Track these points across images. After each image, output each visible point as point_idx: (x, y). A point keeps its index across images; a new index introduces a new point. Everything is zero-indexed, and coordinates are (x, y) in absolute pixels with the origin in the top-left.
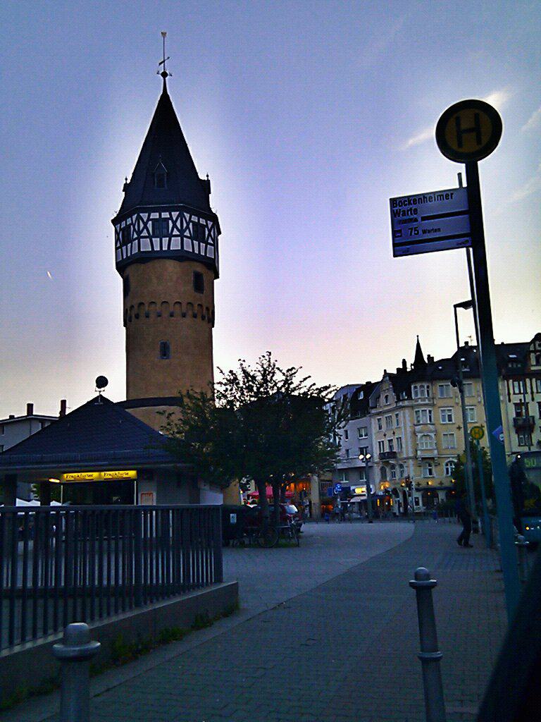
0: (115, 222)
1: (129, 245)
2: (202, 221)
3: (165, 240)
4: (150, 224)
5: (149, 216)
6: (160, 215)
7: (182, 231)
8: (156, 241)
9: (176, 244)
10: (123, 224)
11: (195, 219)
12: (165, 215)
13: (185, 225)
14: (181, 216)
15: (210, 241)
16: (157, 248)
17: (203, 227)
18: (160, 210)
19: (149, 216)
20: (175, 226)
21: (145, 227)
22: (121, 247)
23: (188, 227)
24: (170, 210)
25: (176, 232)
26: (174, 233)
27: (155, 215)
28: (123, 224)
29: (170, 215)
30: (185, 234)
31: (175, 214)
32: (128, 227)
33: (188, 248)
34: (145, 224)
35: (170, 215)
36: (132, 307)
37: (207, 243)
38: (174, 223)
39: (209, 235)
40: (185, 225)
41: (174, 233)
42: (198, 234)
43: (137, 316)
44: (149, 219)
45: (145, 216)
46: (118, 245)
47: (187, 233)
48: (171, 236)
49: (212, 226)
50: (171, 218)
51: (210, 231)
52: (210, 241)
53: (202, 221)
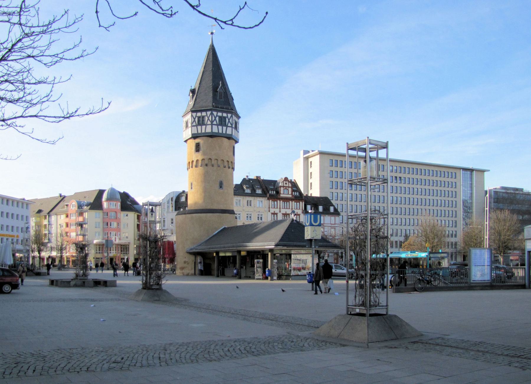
2: (225, 115)
3: (204, 127)
7: (212, 122)
8: (199, 127)
9: (209, 129)
11: (220, 114)
12: (204, 114)
14: (212, 114)
15: (229, 125)
16: (200, 132)
17: (225, 118)
20: (208, 119)
23: (215, 119)
25: (209, 123)
27: (199, 114)
33: (215, 130)
37: (227, 126)
39: (229, 121)
40: (214, 118)
42: (222, 122)
47: (215, 123)
49: (232, 116)
51: (229, 120)
52: (229, 125)
53: (225, 115)
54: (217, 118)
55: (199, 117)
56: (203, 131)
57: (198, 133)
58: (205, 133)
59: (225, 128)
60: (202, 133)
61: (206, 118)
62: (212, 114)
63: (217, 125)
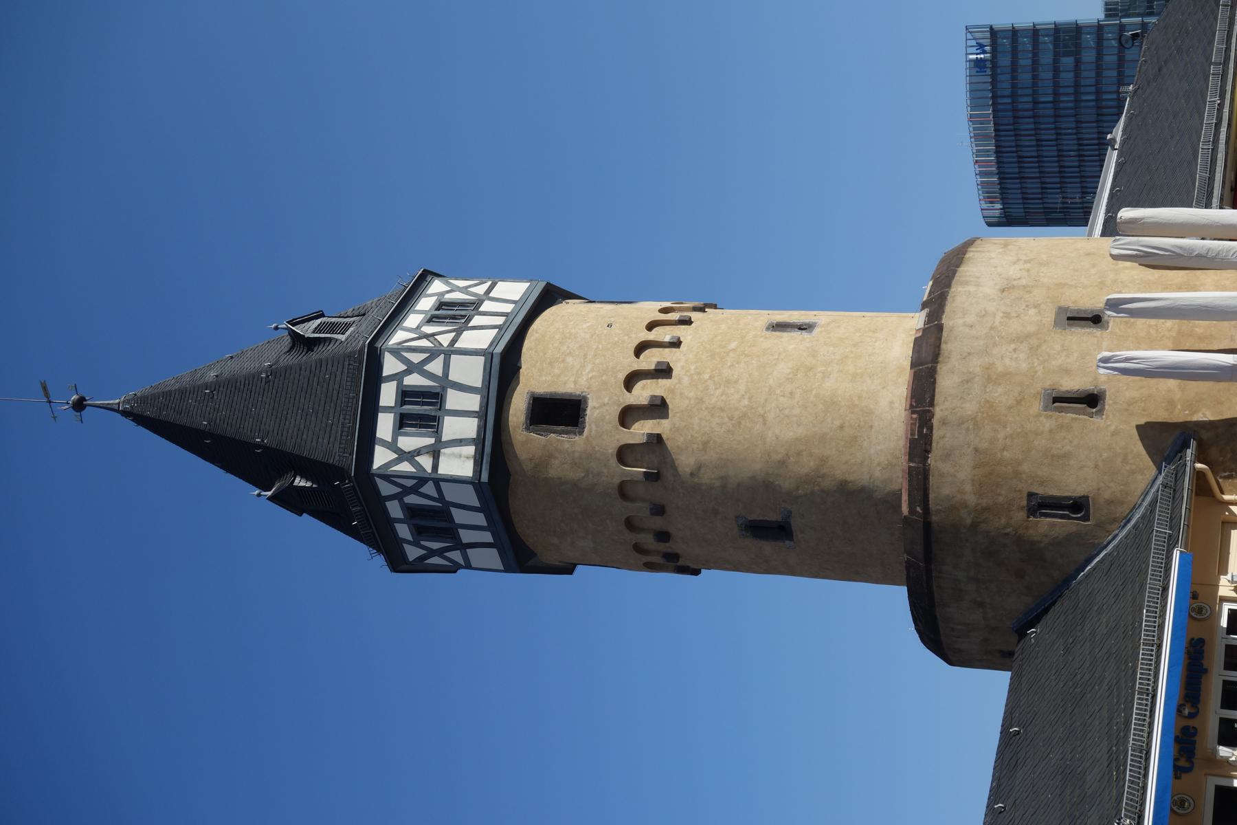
0: (398, 563)
1: (459, 516)
3: (454, 400)
4: (408, 442)
5: (384, 444)
6: (387, 409)
8: (453, 427)
9: (469, 371)
10: (403, 531)
12: (388, 396)
13: (425, 343)
14: (396, 352)
16: (469, 428)
17: (441, 305)
18: (371, 409)
19: (384, 444)
21: (410, 456)
22: (464, 547)
24: (374, 378)
25: (435, 367)
26: (439, 373)
27: (385, 425)
28: (403, 531)
29: (390, 378)
30: (445, 344)
31: (391, 365)
32: (413, 513)
34: (403, 456)
35: (390, 378)
36: (638, 548)
38: (411, 368)
39: (464, 290)
40: (425, 343)
41: (439, 373)
43: (663, 536)
44: (392, 446)
45: (381, 457)
46: (456, 555)
48: (445, 382)
49: (448, 284)
50: (398, 377)
52: (481, 289)
53: (426, 303)
54: (429, 329)
55: (404, 422)
56: (473, 402)
57: (479, 442)
58: (484, 391)
59: (487, 306)
60: (482, 415)
61: (414, 380)
62: (396, 352)
63: (459, 333)
